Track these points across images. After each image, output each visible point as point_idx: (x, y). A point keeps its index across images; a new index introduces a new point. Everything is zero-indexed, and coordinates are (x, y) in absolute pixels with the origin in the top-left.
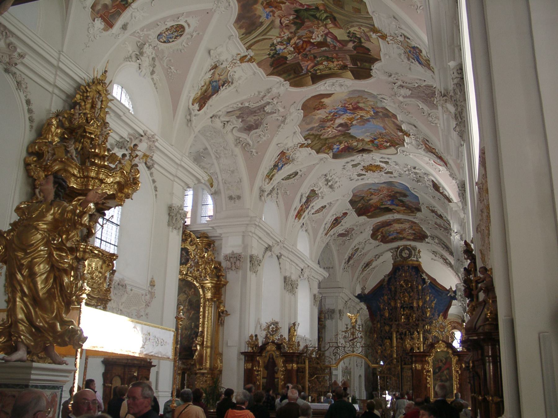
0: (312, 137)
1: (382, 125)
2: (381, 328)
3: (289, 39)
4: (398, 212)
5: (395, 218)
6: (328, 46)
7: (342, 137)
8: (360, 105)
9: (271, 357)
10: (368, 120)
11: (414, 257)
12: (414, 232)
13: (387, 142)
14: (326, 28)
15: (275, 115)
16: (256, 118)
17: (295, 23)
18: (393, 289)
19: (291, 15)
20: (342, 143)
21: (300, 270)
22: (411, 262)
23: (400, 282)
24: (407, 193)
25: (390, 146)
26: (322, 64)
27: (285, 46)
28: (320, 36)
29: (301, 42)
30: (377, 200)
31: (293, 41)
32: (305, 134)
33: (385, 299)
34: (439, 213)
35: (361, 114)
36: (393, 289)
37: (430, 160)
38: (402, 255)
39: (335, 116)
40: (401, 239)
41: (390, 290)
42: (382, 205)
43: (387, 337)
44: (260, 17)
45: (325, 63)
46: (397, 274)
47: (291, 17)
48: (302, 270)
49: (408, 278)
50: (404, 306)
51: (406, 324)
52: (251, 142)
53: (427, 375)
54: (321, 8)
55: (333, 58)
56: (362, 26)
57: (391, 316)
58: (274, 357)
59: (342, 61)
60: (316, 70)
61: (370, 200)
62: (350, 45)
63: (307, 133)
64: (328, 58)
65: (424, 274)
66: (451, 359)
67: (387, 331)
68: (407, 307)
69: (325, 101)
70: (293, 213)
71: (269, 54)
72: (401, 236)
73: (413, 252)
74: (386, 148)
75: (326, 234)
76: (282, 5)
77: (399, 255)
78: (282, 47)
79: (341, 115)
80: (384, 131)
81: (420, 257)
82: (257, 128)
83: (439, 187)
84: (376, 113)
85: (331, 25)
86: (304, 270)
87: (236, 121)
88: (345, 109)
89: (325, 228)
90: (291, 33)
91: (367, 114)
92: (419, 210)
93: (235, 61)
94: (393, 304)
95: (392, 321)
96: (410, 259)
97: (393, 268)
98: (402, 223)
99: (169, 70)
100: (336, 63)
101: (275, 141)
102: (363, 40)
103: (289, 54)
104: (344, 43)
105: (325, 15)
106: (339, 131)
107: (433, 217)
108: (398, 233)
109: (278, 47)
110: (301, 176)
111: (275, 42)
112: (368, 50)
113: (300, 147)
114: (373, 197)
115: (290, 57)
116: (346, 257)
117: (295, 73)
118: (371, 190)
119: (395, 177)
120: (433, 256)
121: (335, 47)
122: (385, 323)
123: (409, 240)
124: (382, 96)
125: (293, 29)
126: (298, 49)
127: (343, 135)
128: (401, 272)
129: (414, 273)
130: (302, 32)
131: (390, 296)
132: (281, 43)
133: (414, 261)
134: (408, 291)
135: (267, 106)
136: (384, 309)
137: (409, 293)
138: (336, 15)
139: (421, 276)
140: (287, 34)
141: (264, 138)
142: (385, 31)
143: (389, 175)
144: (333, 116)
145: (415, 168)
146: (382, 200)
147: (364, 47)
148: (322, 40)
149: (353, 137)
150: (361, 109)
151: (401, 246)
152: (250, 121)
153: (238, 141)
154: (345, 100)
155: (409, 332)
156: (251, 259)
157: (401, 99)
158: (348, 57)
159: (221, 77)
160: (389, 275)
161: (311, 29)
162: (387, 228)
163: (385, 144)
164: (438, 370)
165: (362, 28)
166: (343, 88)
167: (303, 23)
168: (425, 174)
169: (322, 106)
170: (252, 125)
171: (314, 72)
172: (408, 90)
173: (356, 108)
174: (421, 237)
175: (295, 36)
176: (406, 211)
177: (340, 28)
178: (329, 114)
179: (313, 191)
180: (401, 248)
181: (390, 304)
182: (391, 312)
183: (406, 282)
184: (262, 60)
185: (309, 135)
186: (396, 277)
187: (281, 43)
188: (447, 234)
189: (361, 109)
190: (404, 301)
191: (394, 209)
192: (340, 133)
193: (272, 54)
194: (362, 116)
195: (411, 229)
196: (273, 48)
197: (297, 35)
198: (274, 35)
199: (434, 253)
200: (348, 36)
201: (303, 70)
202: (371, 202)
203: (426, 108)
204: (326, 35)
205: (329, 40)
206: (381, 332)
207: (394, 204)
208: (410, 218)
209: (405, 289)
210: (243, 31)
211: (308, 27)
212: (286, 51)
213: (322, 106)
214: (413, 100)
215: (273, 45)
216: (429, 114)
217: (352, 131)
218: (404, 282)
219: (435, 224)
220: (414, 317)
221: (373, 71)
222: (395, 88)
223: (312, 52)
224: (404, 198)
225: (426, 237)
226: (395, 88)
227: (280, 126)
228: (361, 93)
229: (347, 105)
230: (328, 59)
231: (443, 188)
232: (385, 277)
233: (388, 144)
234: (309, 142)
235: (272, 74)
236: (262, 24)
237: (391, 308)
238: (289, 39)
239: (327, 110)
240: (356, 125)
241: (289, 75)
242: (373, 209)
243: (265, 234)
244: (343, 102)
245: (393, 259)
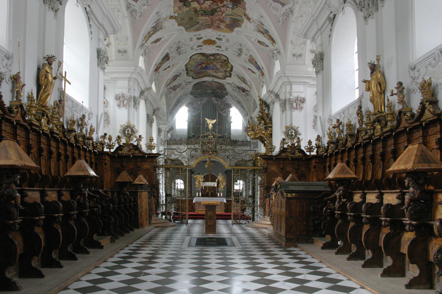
14: (201, 7)
17: (216, 11)
19: (216, 15)
28: (206, 3)
29: (218, 3)
31: (222, 5)
44: (230, 20)
47: (216, 14)
54: (200, 15)
56: (182, 13)
76: (217, 19)
78: (229, 5)
85: (198, 8)
90: (220, 8)
102: (183, 5)
105: (199, 13)
109: (231, 7)
111: (230, 9)
125: (218, 10)
130: (215, 7)
132: (228, 7)
138: (194, 13)
140: (222, 9)
161: (210, 7)
167: (212, 10)
187: (228, 7)
196: (233, 8)
197: (218, 7)
198: (229, 11)
200: (190, 4)
204: (202, 4)
210: (240, 23)
211: (210, 8)
212: (228, 3)
215: (232, 9)
236: (231, 18)
238: (223, 6)
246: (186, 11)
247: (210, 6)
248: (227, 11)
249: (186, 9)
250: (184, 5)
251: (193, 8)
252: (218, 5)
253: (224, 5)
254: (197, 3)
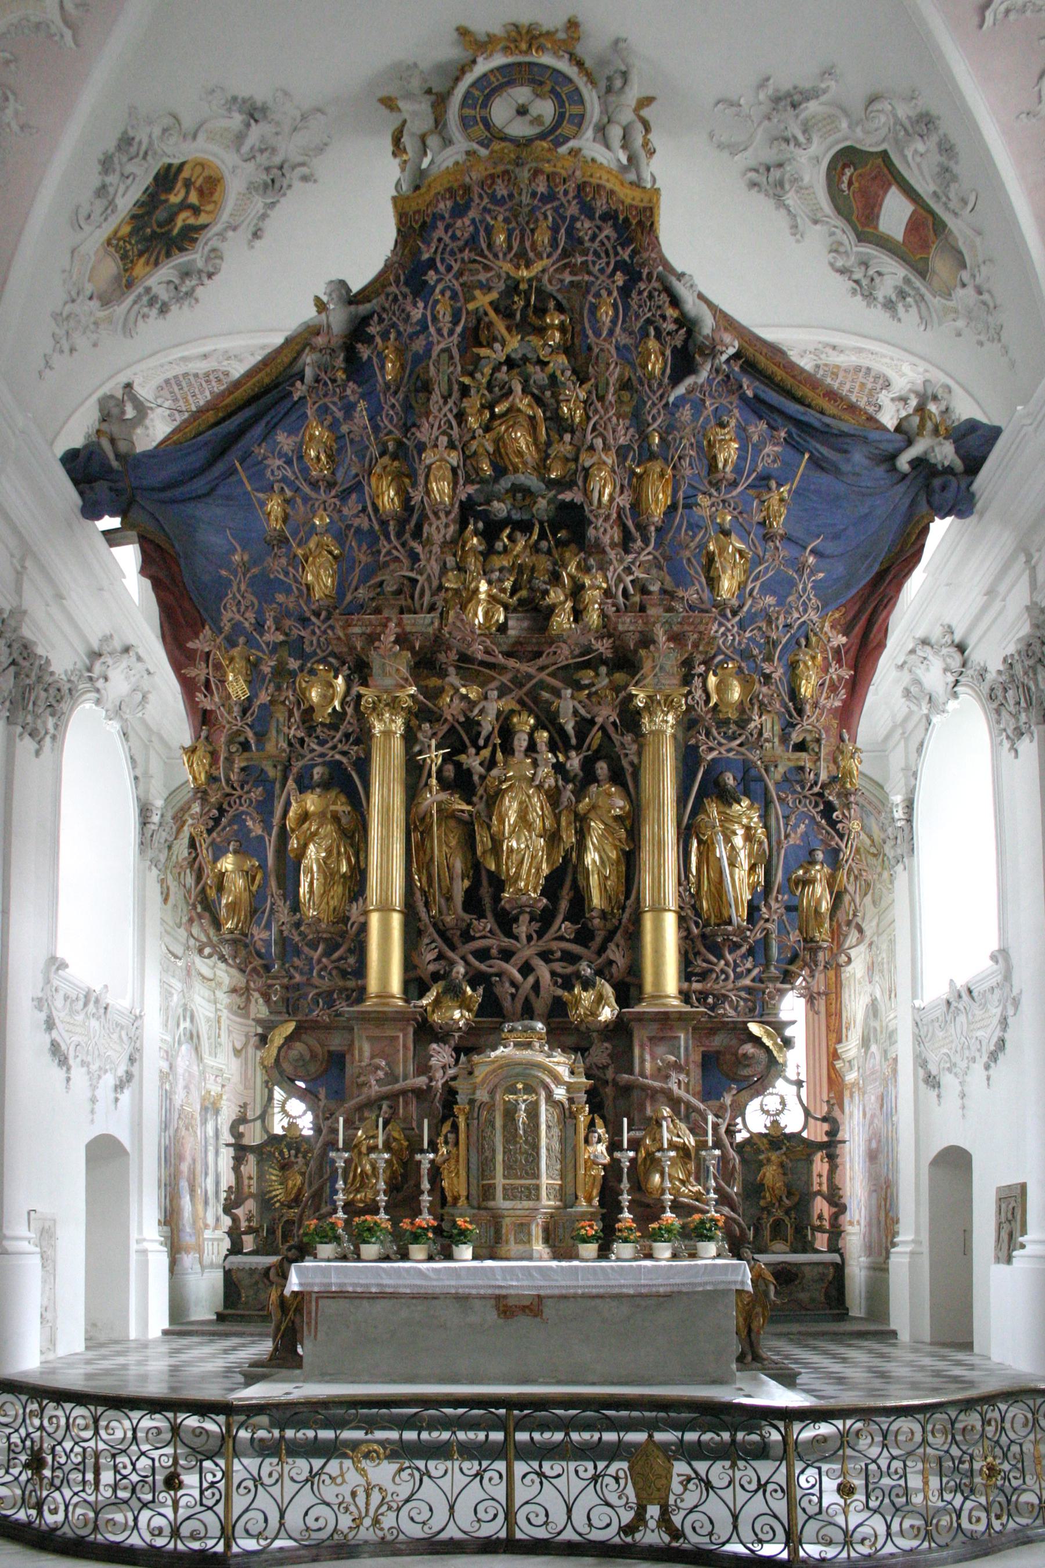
38: (487, 124)
46: (440, 232)
50: (500, 508)
51: (508, 655)
68: (525, 527)
77: (465, 123)
128: (472, 214)
155: (539, 725)
180: (482, 67)
190: (500, 471)
209: (510, 363)
220: (593, 596)
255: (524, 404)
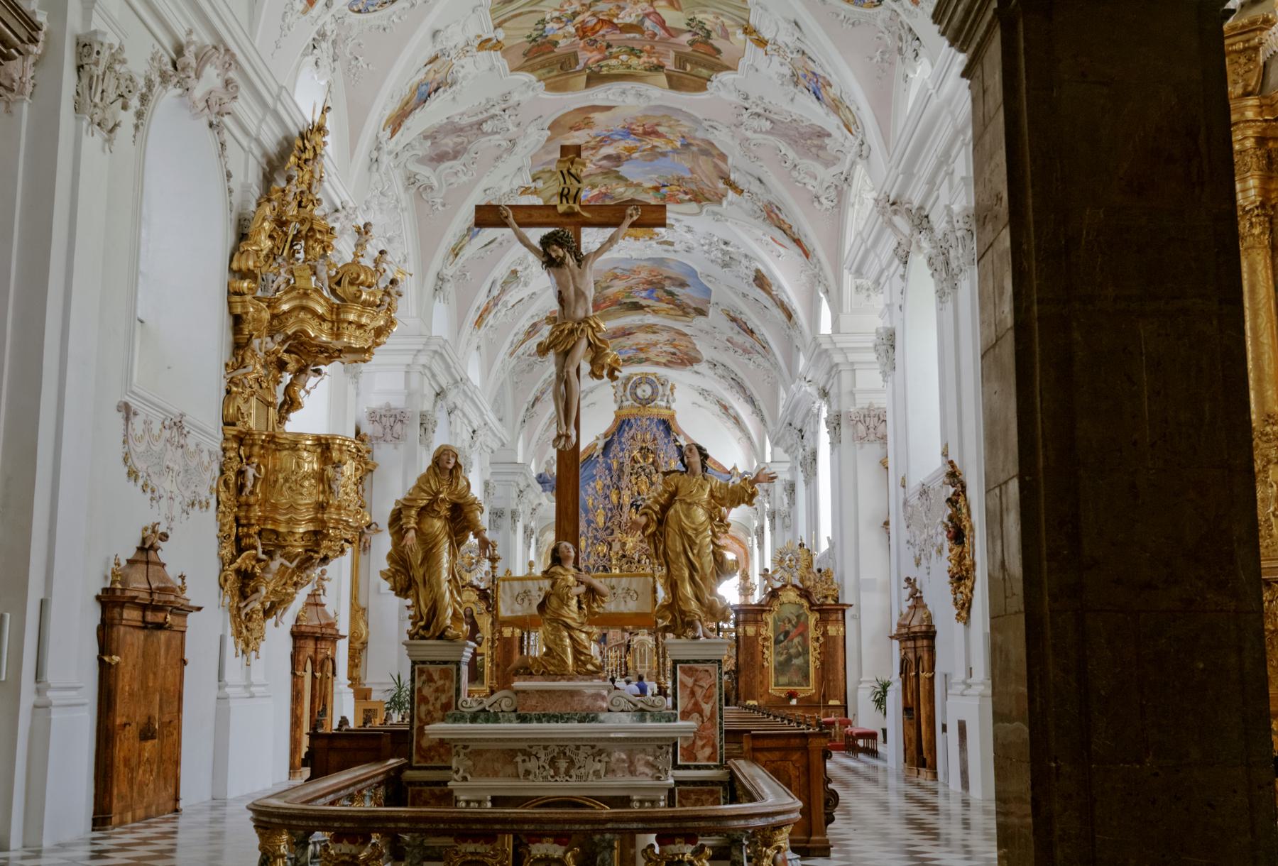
0: (548, 175)
1: (688, 165)
2: (589, 550)
3: (575, 14)
4: (655, 312)
5: (647, 322)
6: (642, 32)
7: (600, 178)
8: (660, 129)
9: (468, 613)
10: (664, 154)
11: (662, 400)
12: (673, 350)
13: (686, 193)
15: (497, 137)
16: (459, 140)
18: (615, 466)
20: (596, 187)
21: (471, 431)
22: (655, 411)
23: (631, 451)
24: (689, 281)
25: (690, 200)
26: (617, 57)
27: (562, 25)
28: (633, 15)
29: (595, 21)
30: (621, 288)
31: (579, 19)
32: (534, 171)
33: (598, 487)
34: (750, 325)
35: (655, 144)
36: (615, 466)
37: (764, 235)
39: (604, 141)
40: (640, 361)
41: (610, 469)
42: (628, 297)
43: (601, 568)
45: (624, 57)
46: (626, 434)
48: (474, 432)
49: (649, 445)
52: (436, 184)
53: (763, 646)
55: (641, 51)
56: (722, 15)
57: (610, 524)
58: (475, 614)
59: (658, 58)
60: (602, 67)
61: (608, 287)
62: (686, 38)
63: (540, 168)
64: (633, 49)
65: (682, 436)
66: (807, 617)
67: (601, 555)
69: (597, 117)
70: (473, 316)
71: (530, 36)
72: (642, 355)
73: (660, 387)
74: (681, 202)
75: (511, 354)
78: (556, 26)
79: (615, 141)
80: (690, 176)
81: (674, 401)
82: (455, 158)
83: (770, 286)
84: (687, 146)
86: (479, 432)
87: (421, 144)
88: (628, 132)
89: (512, 342)
91: (667, 144)
92: (701, 312)
93: (468, 48)
94: (614, 498)
95: (612, 534)
96: (652, 404)
97: (615, 421)
98: (654, 333)
99: (353, 63)
100: (642, 60)
101: (485, 183)
102: (713, 35)
103: (565, 37)
104: (672, 32)
106: (600, 167)
107: (732, 329)
108: (641, 350)
110: (501, 244)
111: (548, 17)
112: (719, 51)
113: (522, 193)
114: (616, 282)
115: (563, 43)
116: (531, 398)
117: (561, 68)
118: (616, 271)
119: (675, 251)
120: (700, 400)
121: (655, 35)
122: (595, 537)
123: (657, 363)
124: (711, 123)
126: (583, 31)
127: (603, 173)
128: (633, 430)
129: (663, 435)
131: (608, 481)
133: (660, 407)
134: (647, 471)
135: (489, 122)
136: (596, 508)
137: (648, 476)
139: (676, 440)
141: (465, 179)
142: (767, 34)
143: (666, 247)
144: (601, 141)
145: (726, 243)
146: (631, 288)
147: (712, 45)
148: (635, 23)
149: (620, 178)
150: (658, 135)
151: (636, 375)
152: (446, 145)
153: (412, 180)
154: (636, 118)
156: (422, 419)
157: (749, 134)
158: (672, 54)
159: (438, 76)
160: (606, 435)
162: (620, 340)
163: (682, 196)
164: (783, 637)
165: (722, 19)
166: (641, 100)
168: (746, 256)
169: (588, 124)
170: (447, 153)
171: (596, 70)
172: (769, 122)
173: (652, 133)
174: (685, 359)
175: (588, 10)
176: (672, 312)
177: (677, 10)
178: (594, 138)
179: (514, 272)
181: (607, 497)
182: (610, 515)
183: (644, 451)
184: (513, 46)
185: (543, 172)
186: (623, 440)
188: (747, 361)
189: (658, 135)
190: (639, 494)
191: (648, 306)
192: (600, 170)
193: (534, 36)
194: (654, 147)
195: (671, 344)
197: (592, 9)
199: (703, 392)
200: (688, 24)
201: (577, 63)
202: (609, 292)
203: (791, 155)
204: (647, 15)
205: (648, 23)
206: (588, 556)
207: (650, 298)
208: (679, 326)
212: (561, 32)
213: (588, 124)
214: (772, 138)
215: (543, 21)
216: (795, 166)
217: (624, 170)
218: (640, 452)
219: (728, 340)
221: (715, 84)
222: (746, 116)
223: (608, 37)
224: (679, 289)
225: (698, 361)
226: (746, 116)
227: (501, 157)
228: (671, 114)
229: (633, 127)
230: (632, 52)
231: (780, 287)
232: (598, 439)
233: (687, 197)
234: (540, 184)
235: (520, 69)
237: (610, 506)
238: (575, 14)
239: (593, 132)
240: (637, 158)
241: (549, 72)
242: (608, 303)
243: (443, 366)
244: (629, 121)
245: (616, 401)
246: (705, 12)
247: (621, 8)
248: (558, 7)
249: (707, 18)
250: (709, 33)
251: (679, 9)
252: (594, 15)
253: (571, 21)
254: (664, 22)
255: (643, 477)
